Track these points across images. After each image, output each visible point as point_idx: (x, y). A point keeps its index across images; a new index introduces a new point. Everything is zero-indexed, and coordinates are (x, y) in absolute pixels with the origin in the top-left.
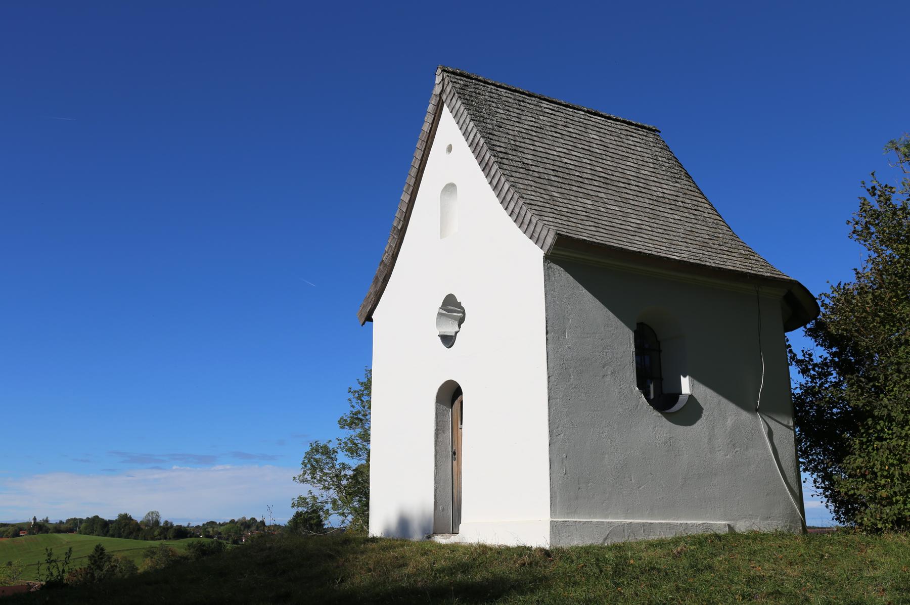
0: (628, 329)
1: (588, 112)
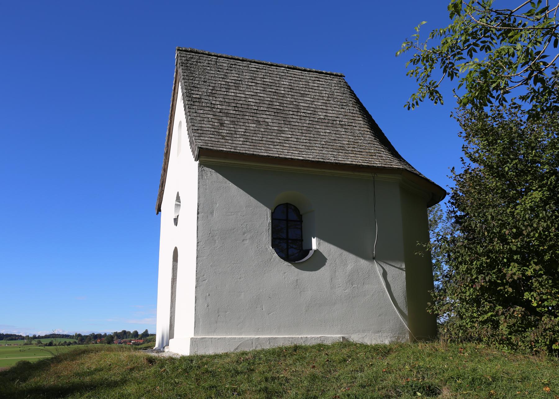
0: (266, 208)
1: (288, 68)
